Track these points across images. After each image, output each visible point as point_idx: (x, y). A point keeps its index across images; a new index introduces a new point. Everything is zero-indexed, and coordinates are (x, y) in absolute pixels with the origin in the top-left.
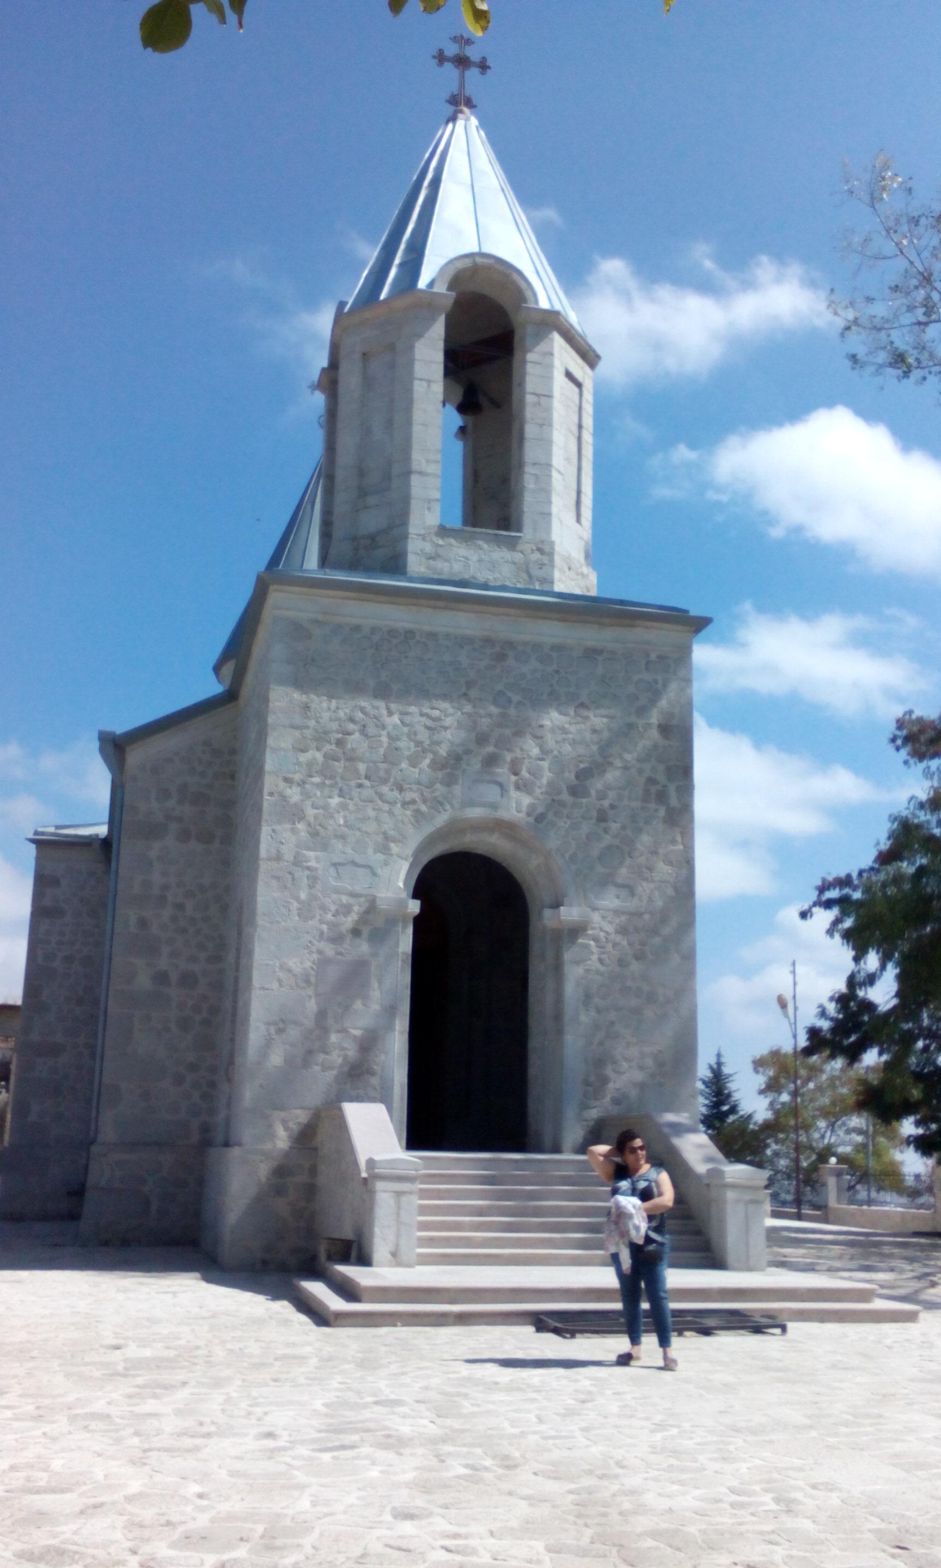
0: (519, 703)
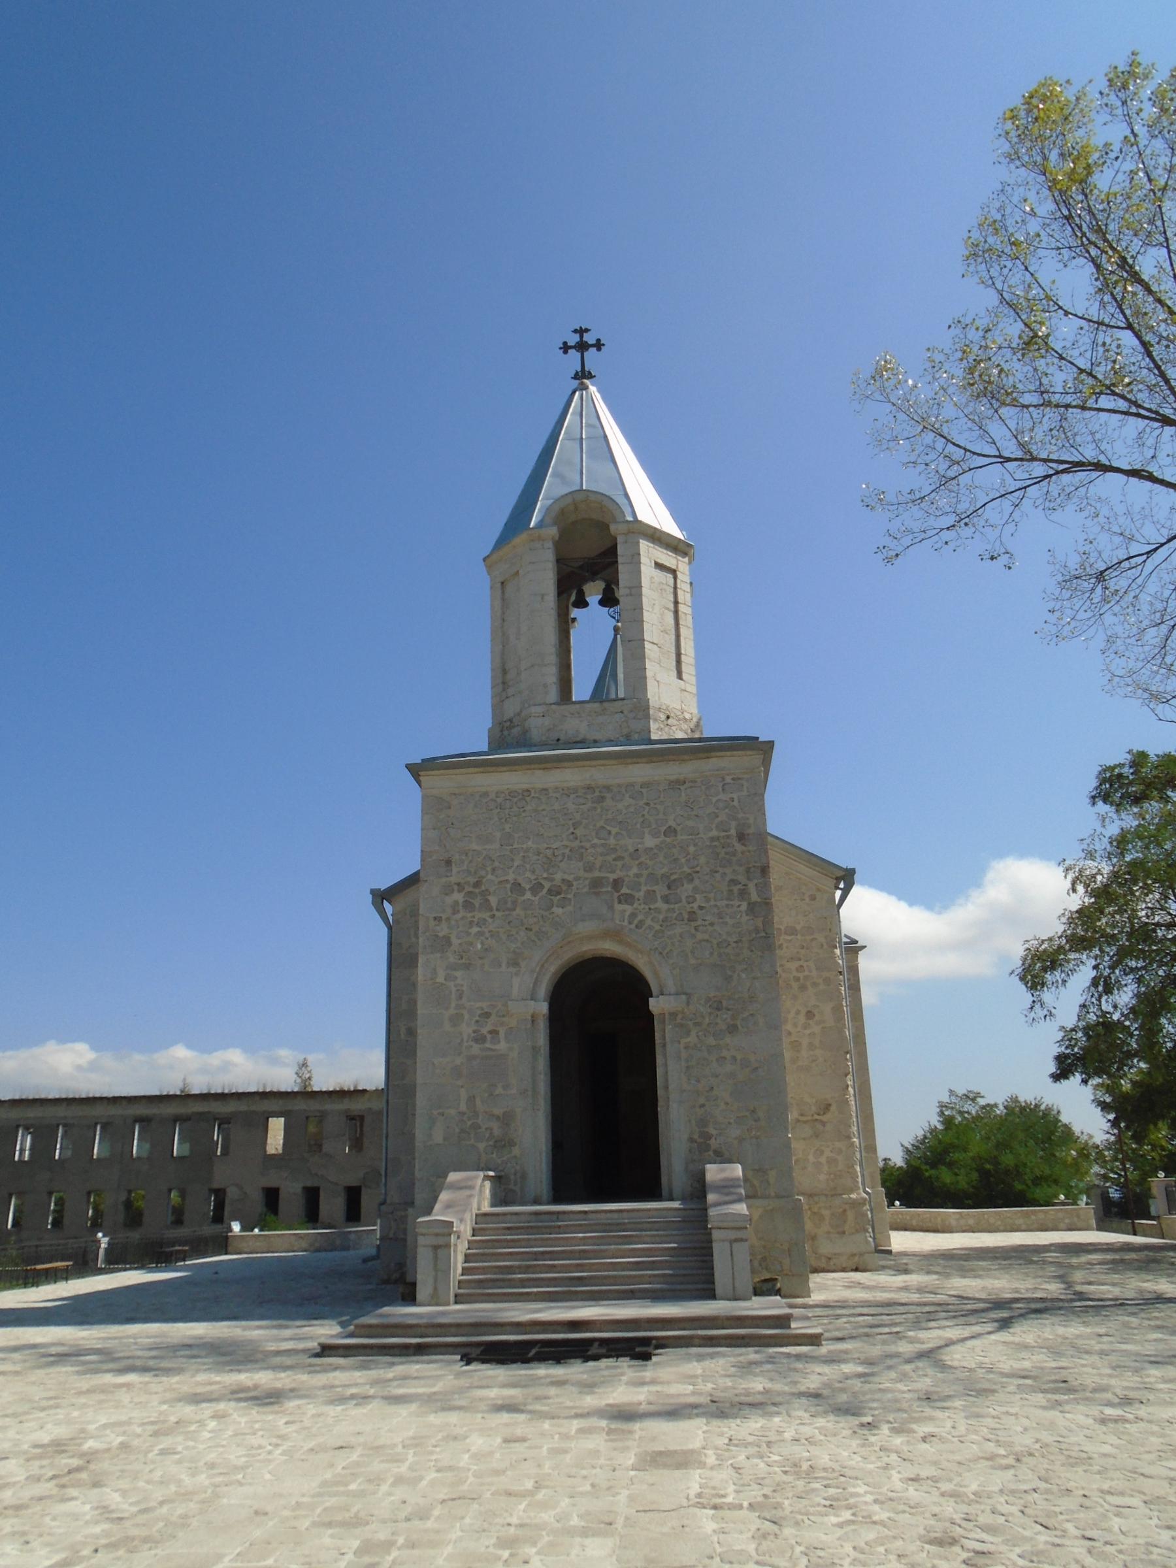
0: (617, 834)
